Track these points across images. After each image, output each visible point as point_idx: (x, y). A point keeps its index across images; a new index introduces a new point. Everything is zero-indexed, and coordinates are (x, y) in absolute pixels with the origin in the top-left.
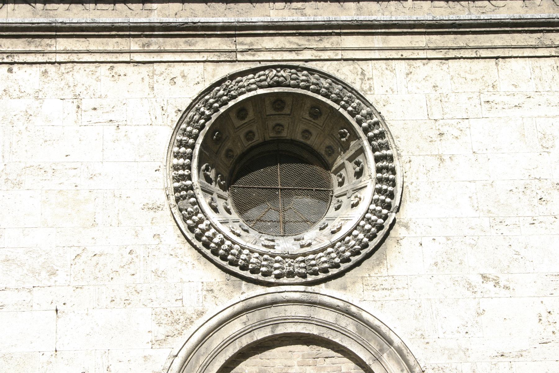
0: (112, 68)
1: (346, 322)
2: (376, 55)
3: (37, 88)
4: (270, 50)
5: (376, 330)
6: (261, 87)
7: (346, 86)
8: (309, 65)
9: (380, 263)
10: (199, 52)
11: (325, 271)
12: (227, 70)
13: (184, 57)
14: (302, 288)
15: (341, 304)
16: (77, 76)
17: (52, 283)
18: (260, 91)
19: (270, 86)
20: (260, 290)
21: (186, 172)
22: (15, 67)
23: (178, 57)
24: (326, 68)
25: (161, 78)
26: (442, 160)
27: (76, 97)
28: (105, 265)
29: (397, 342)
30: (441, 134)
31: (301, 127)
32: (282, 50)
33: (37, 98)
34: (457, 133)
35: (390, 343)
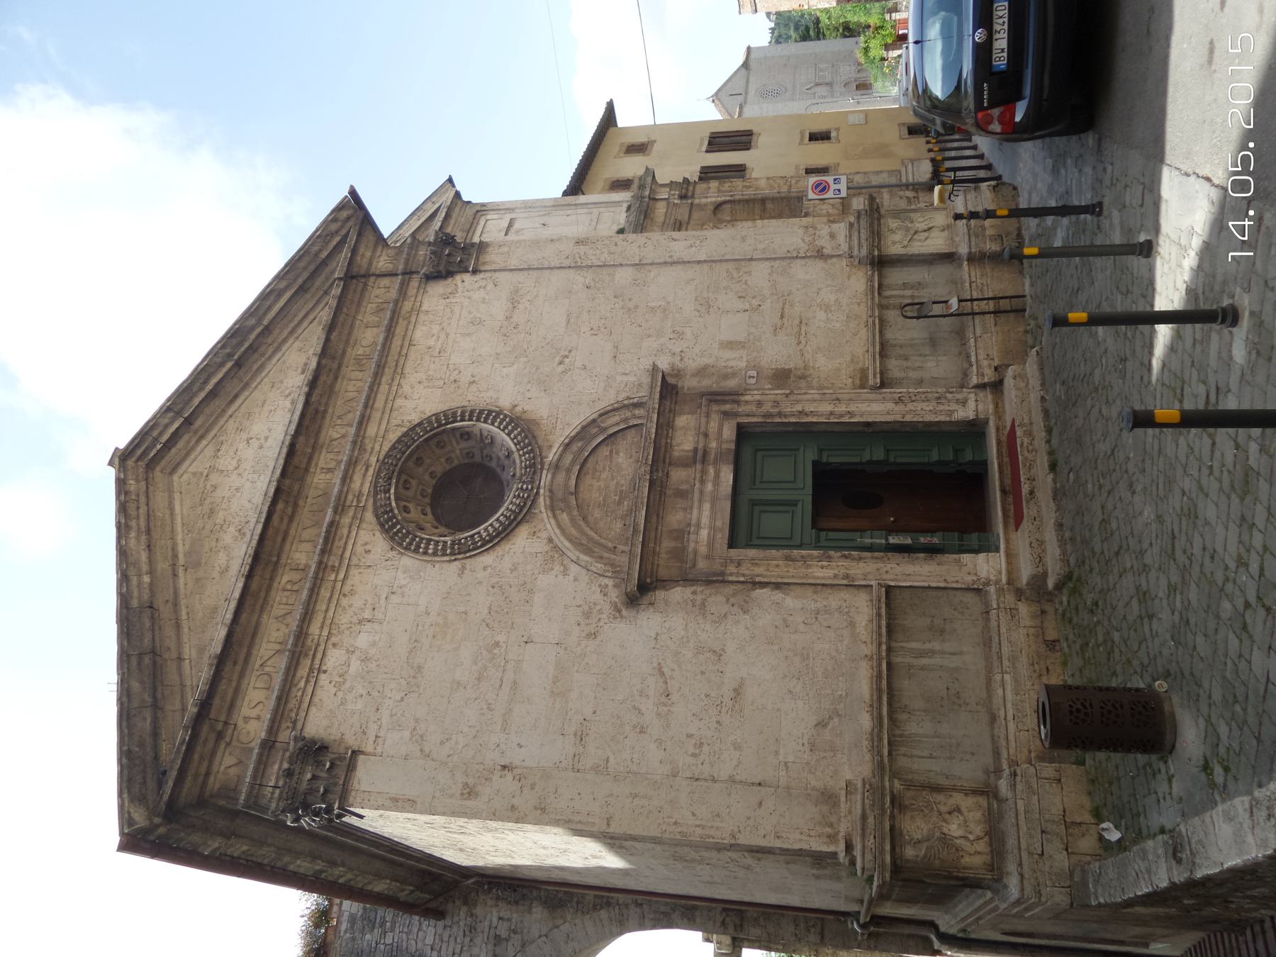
0: (345, 595)
1: (575, 447)
2: (386, 416)
4: (362, 484)
5: (584, 428)
6: (389, 490)
8: (381, 457)
10: (349, 532)
12: (369, 516)
14: (545, 472)
15: (561, 448)
16: (343, 622)
17: (504, 645)
18: (392, 491)
20: (541, 499)
21: (441, 544)
22: (324, 668)
23: (350, 547)
24: (386, 448)
25: (363, 560)
26: (474, 382)
27: (360, 622)
28: (499, 606)
30: (455, 381)
31: (427, 477)
32: (364, 475)
33: (353, 652)
34: (457, 372)
35: (594, 421)
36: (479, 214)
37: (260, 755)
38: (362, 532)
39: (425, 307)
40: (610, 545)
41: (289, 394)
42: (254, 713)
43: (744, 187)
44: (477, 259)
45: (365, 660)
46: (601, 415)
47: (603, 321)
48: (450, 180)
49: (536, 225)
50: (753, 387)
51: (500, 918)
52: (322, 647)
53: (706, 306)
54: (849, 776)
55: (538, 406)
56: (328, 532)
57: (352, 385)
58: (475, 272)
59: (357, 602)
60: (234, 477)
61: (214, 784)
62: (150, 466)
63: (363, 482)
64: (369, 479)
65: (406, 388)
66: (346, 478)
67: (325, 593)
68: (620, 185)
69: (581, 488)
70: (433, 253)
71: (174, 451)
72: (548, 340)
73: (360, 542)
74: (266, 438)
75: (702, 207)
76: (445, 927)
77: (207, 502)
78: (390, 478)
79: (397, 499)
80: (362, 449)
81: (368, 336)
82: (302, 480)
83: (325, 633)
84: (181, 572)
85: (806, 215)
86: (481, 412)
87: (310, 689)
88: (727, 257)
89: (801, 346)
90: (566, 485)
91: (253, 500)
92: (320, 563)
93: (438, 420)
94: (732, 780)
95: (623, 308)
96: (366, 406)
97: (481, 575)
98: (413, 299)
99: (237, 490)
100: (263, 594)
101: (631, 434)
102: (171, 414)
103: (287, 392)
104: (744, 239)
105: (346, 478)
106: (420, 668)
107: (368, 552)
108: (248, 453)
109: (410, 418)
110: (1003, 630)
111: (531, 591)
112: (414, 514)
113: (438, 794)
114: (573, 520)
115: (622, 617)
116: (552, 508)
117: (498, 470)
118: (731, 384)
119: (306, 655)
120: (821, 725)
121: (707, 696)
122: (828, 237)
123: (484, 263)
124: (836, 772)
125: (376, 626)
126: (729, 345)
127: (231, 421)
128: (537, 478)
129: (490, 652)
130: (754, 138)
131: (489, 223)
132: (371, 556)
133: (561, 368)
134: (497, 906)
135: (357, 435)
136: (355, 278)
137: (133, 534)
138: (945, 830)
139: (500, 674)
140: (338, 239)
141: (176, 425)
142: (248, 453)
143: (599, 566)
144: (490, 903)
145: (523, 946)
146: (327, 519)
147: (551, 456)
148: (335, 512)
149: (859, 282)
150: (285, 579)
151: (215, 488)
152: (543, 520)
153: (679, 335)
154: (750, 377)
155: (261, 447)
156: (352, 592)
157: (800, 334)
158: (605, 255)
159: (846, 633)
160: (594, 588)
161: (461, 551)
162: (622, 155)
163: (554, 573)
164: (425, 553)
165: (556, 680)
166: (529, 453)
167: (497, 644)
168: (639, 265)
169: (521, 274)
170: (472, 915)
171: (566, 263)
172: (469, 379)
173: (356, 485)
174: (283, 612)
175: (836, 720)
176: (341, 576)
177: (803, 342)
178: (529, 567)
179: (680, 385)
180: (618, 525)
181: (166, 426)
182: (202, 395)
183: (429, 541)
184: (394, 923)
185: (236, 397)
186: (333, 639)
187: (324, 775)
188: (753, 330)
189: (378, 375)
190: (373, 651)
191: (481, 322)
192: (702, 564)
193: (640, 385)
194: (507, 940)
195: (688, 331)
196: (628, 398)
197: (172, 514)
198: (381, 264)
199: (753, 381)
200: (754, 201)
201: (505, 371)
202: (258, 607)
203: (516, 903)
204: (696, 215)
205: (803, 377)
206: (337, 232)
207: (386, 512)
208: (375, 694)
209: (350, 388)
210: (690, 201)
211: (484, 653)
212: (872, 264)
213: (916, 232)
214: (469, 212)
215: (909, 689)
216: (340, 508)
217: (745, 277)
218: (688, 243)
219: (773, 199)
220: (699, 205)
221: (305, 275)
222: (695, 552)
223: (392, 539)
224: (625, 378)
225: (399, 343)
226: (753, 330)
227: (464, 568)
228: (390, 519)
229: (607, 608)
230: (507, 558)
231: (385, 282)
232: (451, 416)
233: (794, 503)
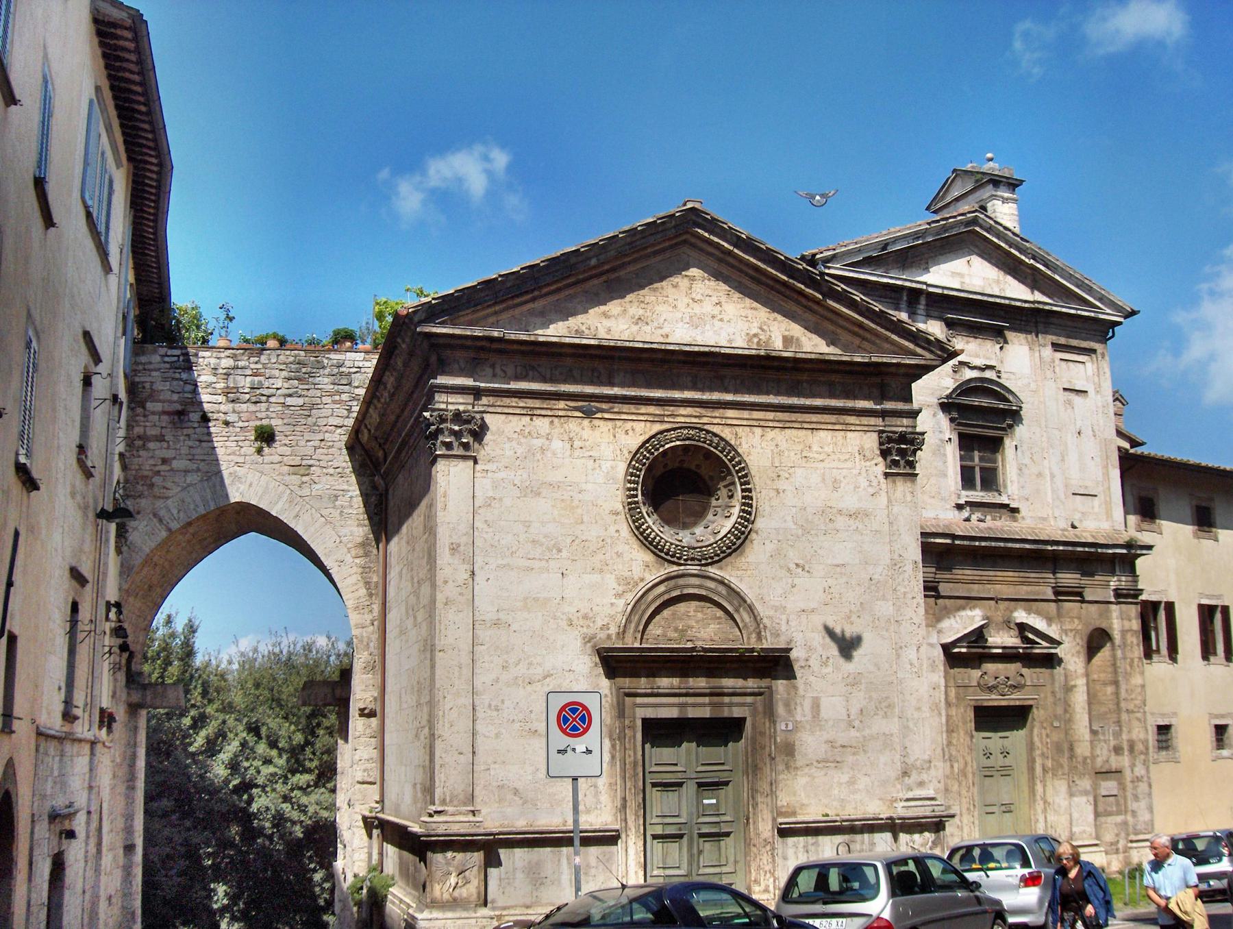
2: (745, 423)
3: (548, 431)
4: (683, 416)
5: (738, 594)
7: (727, 442)
8: (706, 427)
9: (741, 554)
10: (642, 414)
11: (712, 558)
12: (657, 427)
13: (634, 417)
14: (698, 568)
18: (678, 443)
19: (683, 440)
20: (675, 568)
22: (534, 418)
24: (715, 429)
26: (779, 493)
27: (571, 439)
29: (749, 601)
33: (548, 439)
34: (787, 476)
35: (745, 601)
39: (849, 434)
41: (763, 330)
43: (1132, 660)
45: (543, 450)
46: (750, 606)
47: (837, 596)
48: (1133, 313)
49: (1079, 423)
50: (778, 729)
52: (549, 413)
54: (484, 811)
55: (757, 552)
58: (886, 475)
59: (587, 433)
60: (686, 300)
64: (688, 420)
65: (771, 434)
72: (819, 551)
73: (634, 424)
74: (721, 320)
75: (1106, 615)
78: (688, 439)
83: (561, 413)
84: (604, 278)
85: (1094, 733)
87: (518, 411)
89: (815, 764)
91: (666, 323)
95: (851, 611)
97: (612, 529)
98: (858, 423)
99: (675, 307)
103: (765, 327)
104: (919, 709)
108: (708, 307)
109: (743, 443)
111: (601, 571)
113: (451, 526)
115: (586, 643)
117: (705, 522)
118: (780, 710)
120: (516, 792)
121: (531, 712)
122: (919, 780)
123: (894, 482)
124: (486, 803)
125: (568, 453)
126: (816, 706)
129: (554, 546)
132: (624, 436)
138: (453, 875)
142: (708, 307)
147: (713, 571)
152: (659, 571)
154: (787, 725)
155: (713, 317)
156: (593, 427)
157: (827, 762)
158: (903, 590)
160: (606, 619)
163: (615, 585)
165: (536, 600)
167: (560, 551)
172: (781, 488)
177: (820, 765)
178: (620, 567)
179: (779, 668)
186: (556, 420)
188: (831, 723)
190: (549, 454)
191: (836, 489)
194: (334, 508)
195: (830, 669)
196: (765, 627)
199: (783, 727)
200: (1115, 672)
201: (789, 518)
208: (518, 462)
211: (553, 542)
217: (881, 713)
218: (915, 662)
224: (783, 622)
226: (831, 723)
229: (591, 632)
230: (627, 547)
232: (745, 479)
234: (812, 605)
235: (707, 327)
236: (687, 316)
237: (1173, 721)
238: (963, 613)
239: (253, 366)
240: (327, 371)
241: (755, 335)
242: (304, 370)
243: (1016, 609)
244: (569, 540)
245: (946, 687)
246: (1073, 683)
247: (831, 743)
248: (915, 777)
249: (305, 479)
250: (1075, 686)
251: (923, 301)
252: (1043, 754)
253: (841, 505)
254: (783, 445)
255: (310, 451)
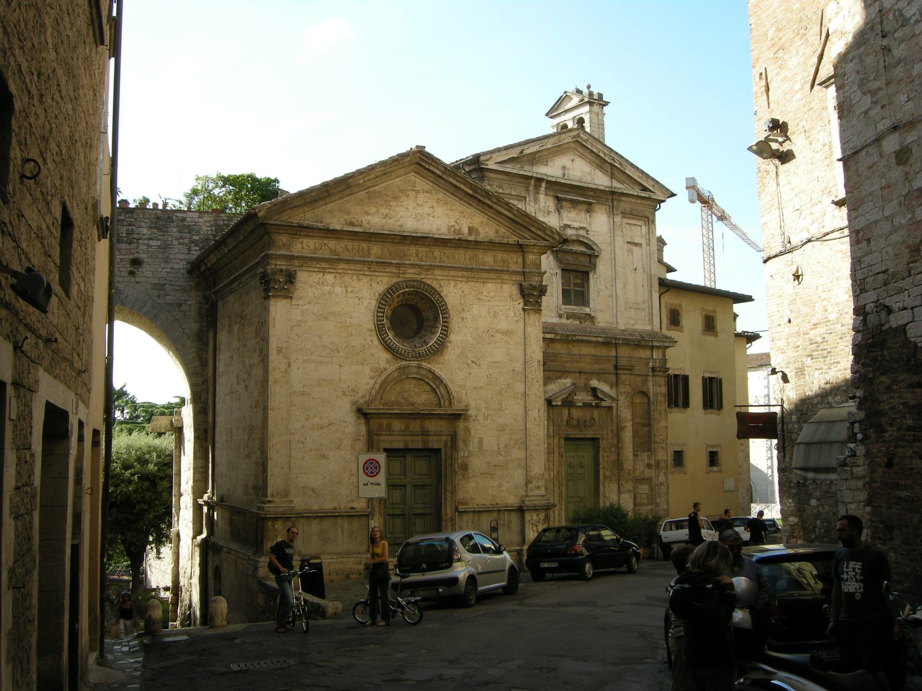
5: (439, 378)
7: (435, 290)
8: (423, 280)
12: (395, 280)
24: (428, 282)
27: (346, 287)
32: (415, 274)
35: (443, 382)
36: (646, 219)
37: (288, 256)
38: (387, 278)
39: (504, 286)
40: (384, 397)
41: (457, 223)
42: (305, 246)
44: (532, 309)
45: (330, 293)
46: (445, 385)
48: (673, 195)
51: (190, 305)
52: (334, 271)
53: (502, 429)
55: (451, 353)
56: (387, 263)
57: (462, 257)
58: (524, 309)
59: (355, 283)
60: (413, 205)
61: (276, 237)
62: (417, 163)
63: (411, 274)
65: (460, 285)
66: (413, 265)
67: (358, 267)
68: (675, 319)
69: (410, 380)
70: (535, 287)
71: (426, 171)
73: (382, 278)
74: (433, 217)
75: (645, 382)
76: (183, 274)
77: (401, 194)
79: (403, 293)
80: (428, 270)
81: (488, 259)
82: (412, 243)
85: (635, 455)
86: (447, 327)
88: (528, 438)
90: (411, 373)
92: (372, 262)
93: (443, 306)
94: (291, 456)
96: (450, 267)
97: (369, 340)
99: (407, 208)
100: (357, 238)
101: (435, 400)
102: (443, 170)
104: (538, 445)
105: (413, 265)
106: (327, 319)
107: (378, 283)
108: (426, 209)
110: (353, 559)
111: (362, 364)
112: (396, 300)
114: (395, 378)
116: (400, 368)
117: (420, 335)
118: (461, 444)
119: (330, 265)
120: (313, 490)
123: (529, 314)
125: (344, 294)
126: (481, 442)
127: (443, 195)
128: (414, 359)
130: (715, 411)
131: (639, 228)
132: (376, 285)
133: (470, 362)
134: (197, 303)
135: (435, 266)
136: (521, 248)
137: (382, 169)
139: (326, 355)
140: (542, 235)
141: (438, 172)
142: (426, 209)
143: (374, 393)
144: (198, 299)
145: (177, 320)
146: (393, 261)
147: (425, 365)
148: (396, 264)
149: (512, 500)
150: (364, 245)
151: (408, 196)
153: (486, 418)
156: (359, 280)
159: (349, 499)
161: (380, 330)
162: (704, 313)
164: (378, 312)
165: (325, 380)
166: (427, 354)
167: (339, 352)
168: (525, 395)
169: (523, 334)
170: (190, 289)
171: (528, 357)
173: (410, 271)
174: (349, 247)
175: (315, 496)
176: (366, 273)
180: (393, 399)
181: (438, 168)
182: (454, 182)
183: (384, 313)
184: (184, 244)
185: (455, 196)
187: (282, 285)
188: (488, 452)
189: (467, 269)
192: (375, 437)
193: (461, 402)
194: (180, 311)
195: (489, 422)
196: (454, 397)
197: (394, 179)
198: (531, 257)
199: (462, 454)
201: (468, 335)
202: (351, 237)
203: (199, 314)
204: (639, 379)
205: (464, 477)
206: (546, 234)
207: (396, 288)
209: (460, 255)
210: (651, 374)
212: (521, 506)
213: (537, 526)
214: (647, 213)
215: (328, 523)
216: (398, 266)
217: (517, 447)
219: (650, 432)
220: (647, 381)
221: (521, 222)
222: (381, 435)
223: (385, 294)
225: (485, 277)
226: (488, 452)
227: (371, 330)
228: (394, 292)
229: (355, 399)
231: (520, 260)
232: (446, 311)
233: (405, 475)
234: (481, 384)
235: (425, 221)
236: (414, 214)
237: (684, 449)
238: (560, 381)
239: (128, 220)
240: (175, 224)
241: (453, 226)
242: (160, 223)
243: (592, 379)
244: (344, 346)
245: (548, 426)
246: (624, 425)
247: (488, 463)
248: (534, 483)
249: (162, 292)
250: (625, 427)
251: (543, 185)
252: (604, 468)
253: (498, 327)
254: (467, 291)
255: (165, 275)
